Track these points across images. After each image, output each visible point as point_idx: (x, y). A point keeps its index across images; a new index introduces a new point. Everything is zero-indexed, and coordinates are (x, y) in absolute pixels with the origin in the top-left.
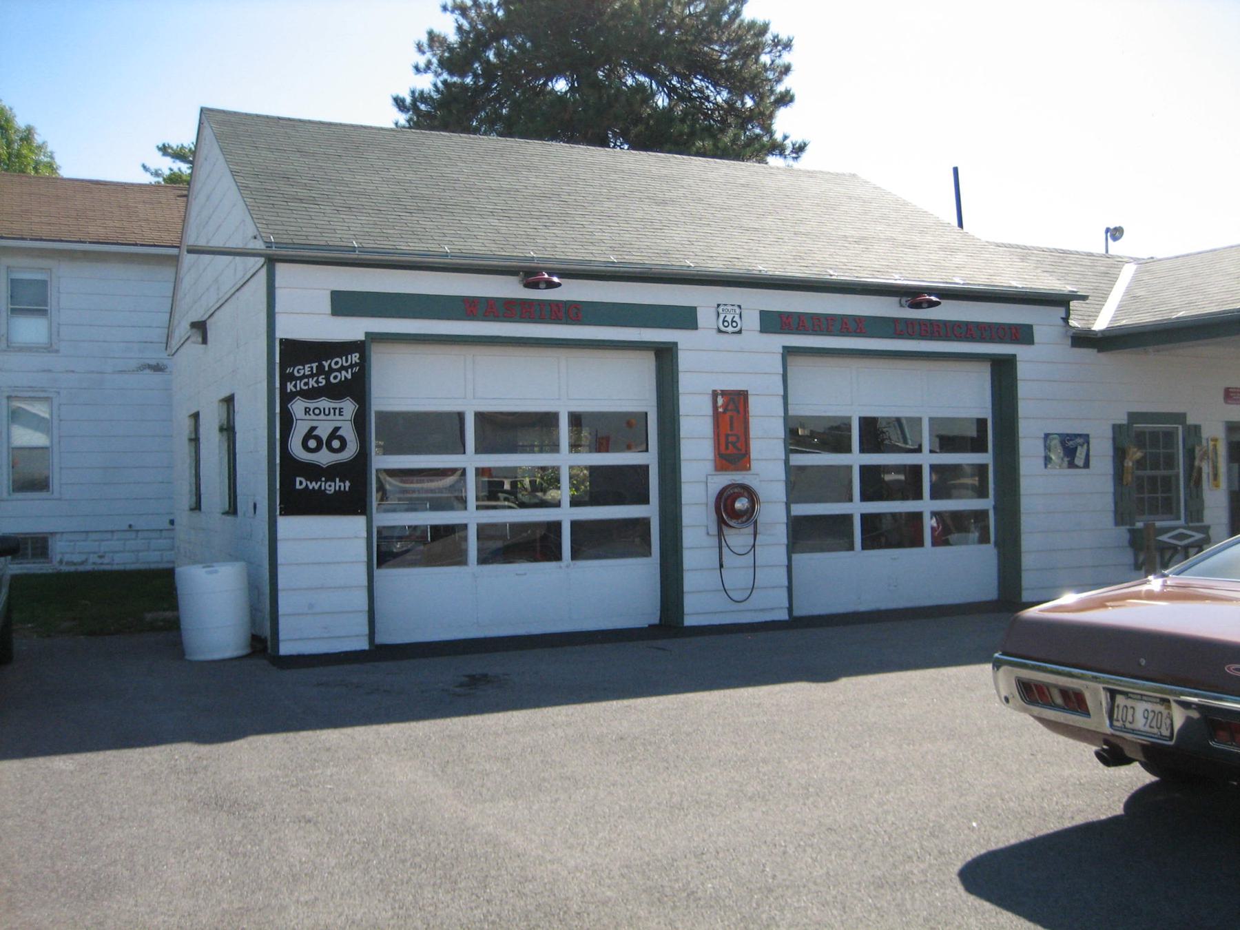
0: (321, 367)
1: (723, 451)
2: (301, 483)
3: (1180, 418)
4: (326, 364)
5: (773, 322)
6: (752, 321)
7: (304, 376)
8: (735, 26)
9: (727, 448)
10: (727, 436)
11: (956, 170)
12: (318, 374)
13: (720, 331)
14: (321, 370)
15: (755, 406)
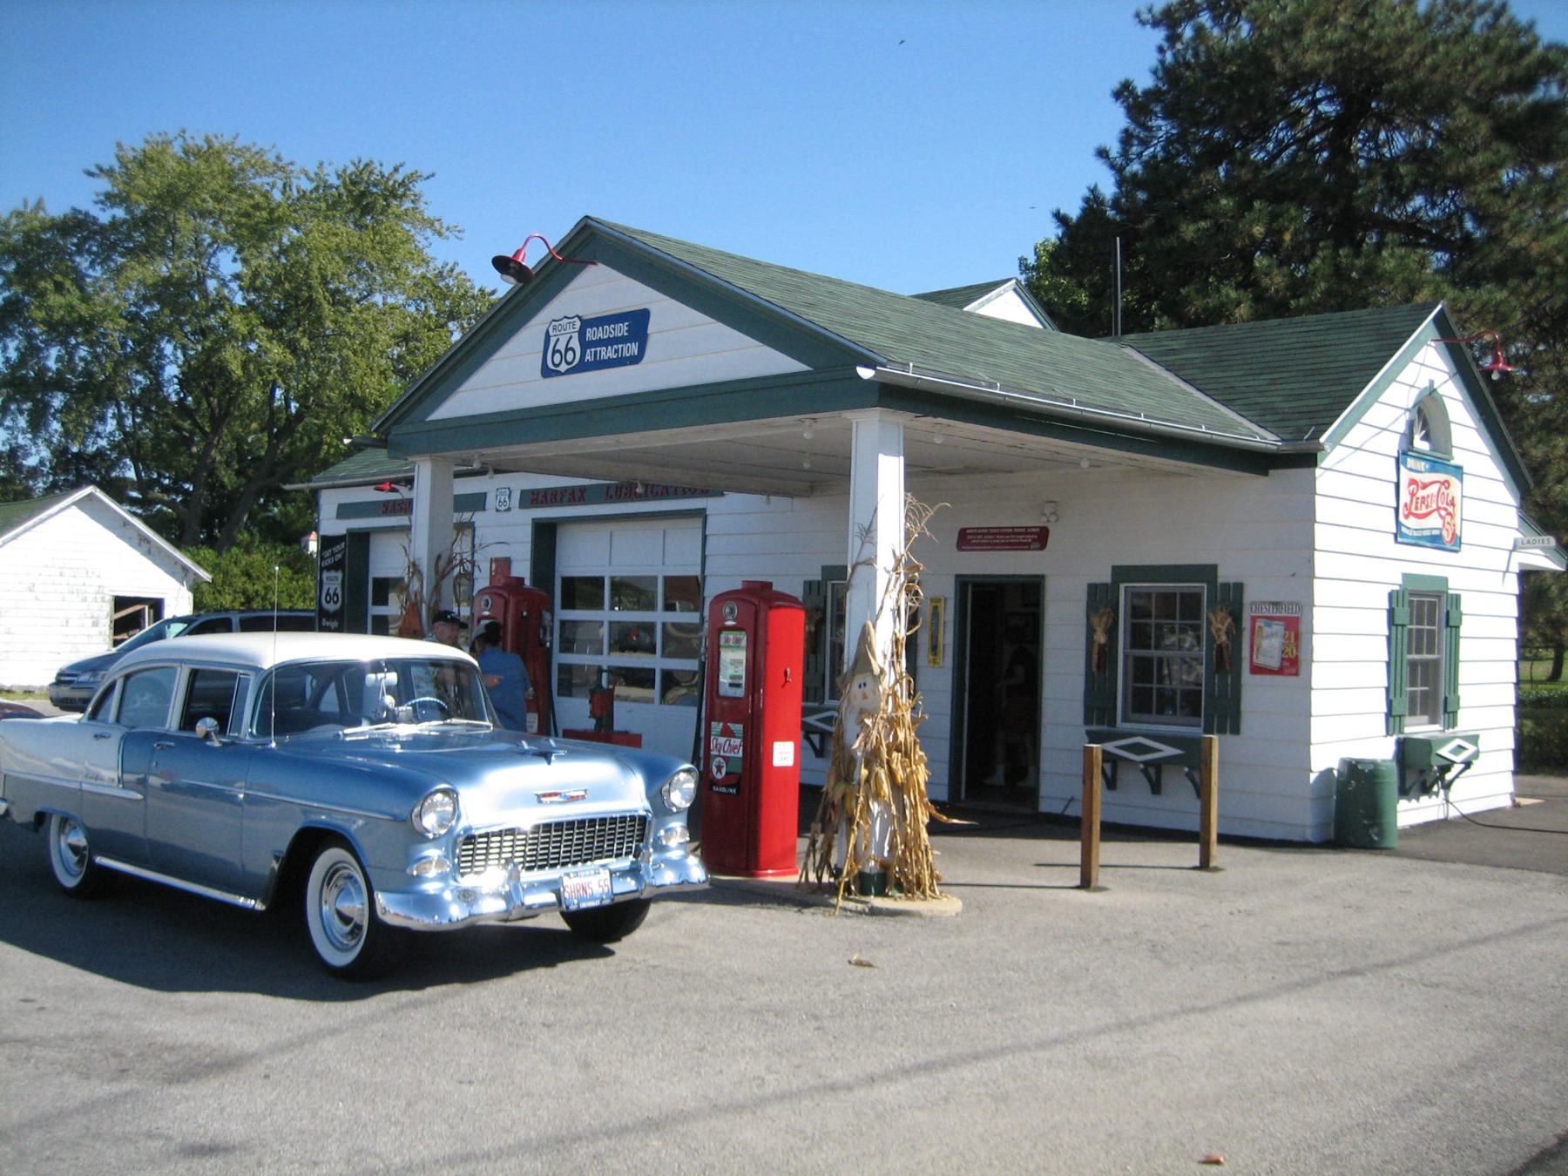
5: (532, 498)
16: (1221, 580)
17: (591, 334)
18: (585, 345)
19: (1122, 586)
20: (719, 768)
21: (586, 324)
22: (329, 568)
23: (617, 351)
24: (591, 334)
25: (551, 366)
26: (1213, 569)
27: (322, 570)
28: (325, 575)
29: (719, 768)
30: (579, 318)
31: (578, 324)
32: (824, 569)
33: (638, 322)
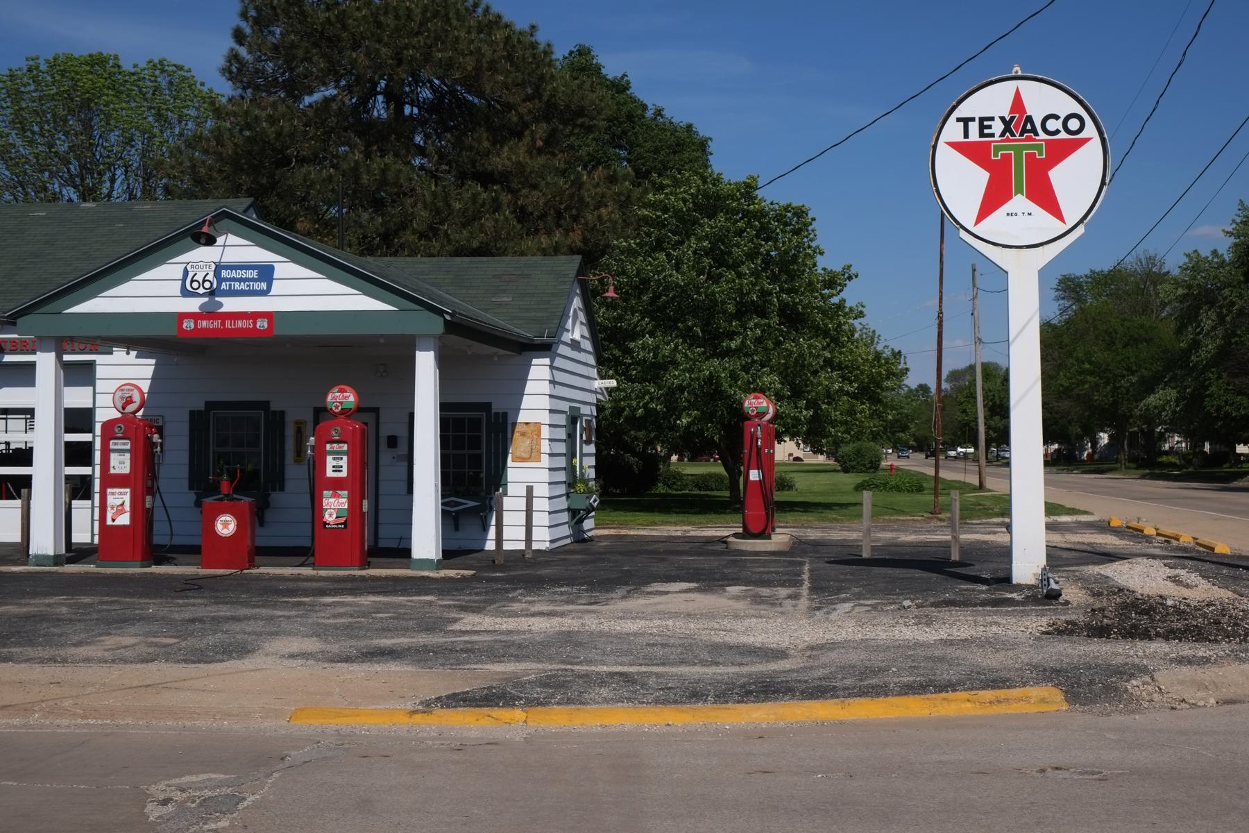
3: (265, 405)
8: (480, 10)
16: (493, 411)
18: (220, 280)
20: (331, 515)
23: (248, 286)
24: (224, 273)
29: (331, 515)
30: (215, 263)
31: (213, 266)
32: (207, 403)
33: (266, 273)
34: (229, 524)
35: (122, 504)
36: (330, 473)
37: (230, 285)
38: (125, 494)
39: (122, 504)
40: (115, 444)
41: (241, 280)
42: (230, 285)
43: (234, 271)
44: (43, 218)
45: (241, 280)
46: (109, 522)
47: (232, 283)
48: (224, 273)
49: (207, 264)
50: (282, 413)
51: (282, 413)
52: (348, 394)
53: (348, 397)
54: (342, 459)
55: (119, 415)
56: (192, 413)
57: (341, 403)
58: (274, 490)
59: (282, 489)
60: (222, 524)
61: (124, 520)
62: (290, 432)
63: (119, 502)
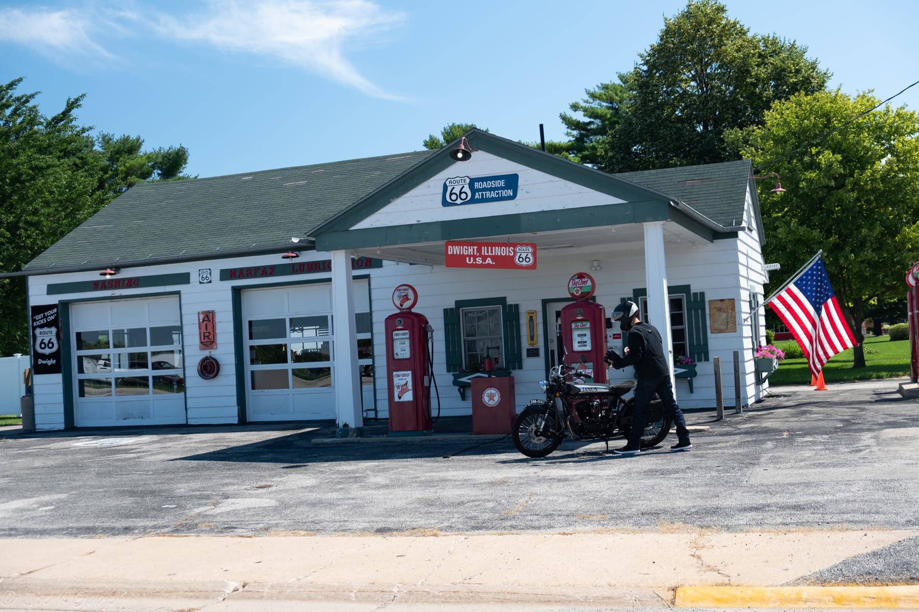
0: (44, 315)
1: (203, 341)
2: (40, 361)
3: (502, 301)
4: (46, 314)
5: (228, 275)
6: (216, 275)
7: (39, 319)
9: (204, 339)
10: (204, 333)
11: (541, 126)
12: (43, 318)
13: (200, 283)
14: (45, 317)
15: (218, 318)
16: (692, 292)
17: (477, 185)
19: (639, 298)
21: (472, 181)
22: (41, 326)
23: (497, 194)
24: (477, 185)
25: (449, 200)
26: (688, 287)
27: (34, 328)
28: (38, 331)
31: (468, 181)
32: (456, 302)
33: (512, 181)
34: (494, 396)
35: (406, 384)
36: (576, 347)
37: (482, 194)
38: (407, 375)
39: (406, 384)
40: (397, 335)
41: (491, 189)
42: (482, 194)
43: (485, 183)
44: (323, 173)
45: (491, 189)
46: (397, 399)
47: (484, 193)
48: (477, 185)
49: (463, 179)
50: (517, 306)
51: (517, 306)
52: (586, 280)
53: (586, 282)
54: (585, 335)
55: (398, 311)
56: (445, 311)
57: (581, 288)
58: (514, 368)
59: (520, 367)
60: (488, 396)
61: (408, 397)
62: (524, 321)
63: (403, 382)
